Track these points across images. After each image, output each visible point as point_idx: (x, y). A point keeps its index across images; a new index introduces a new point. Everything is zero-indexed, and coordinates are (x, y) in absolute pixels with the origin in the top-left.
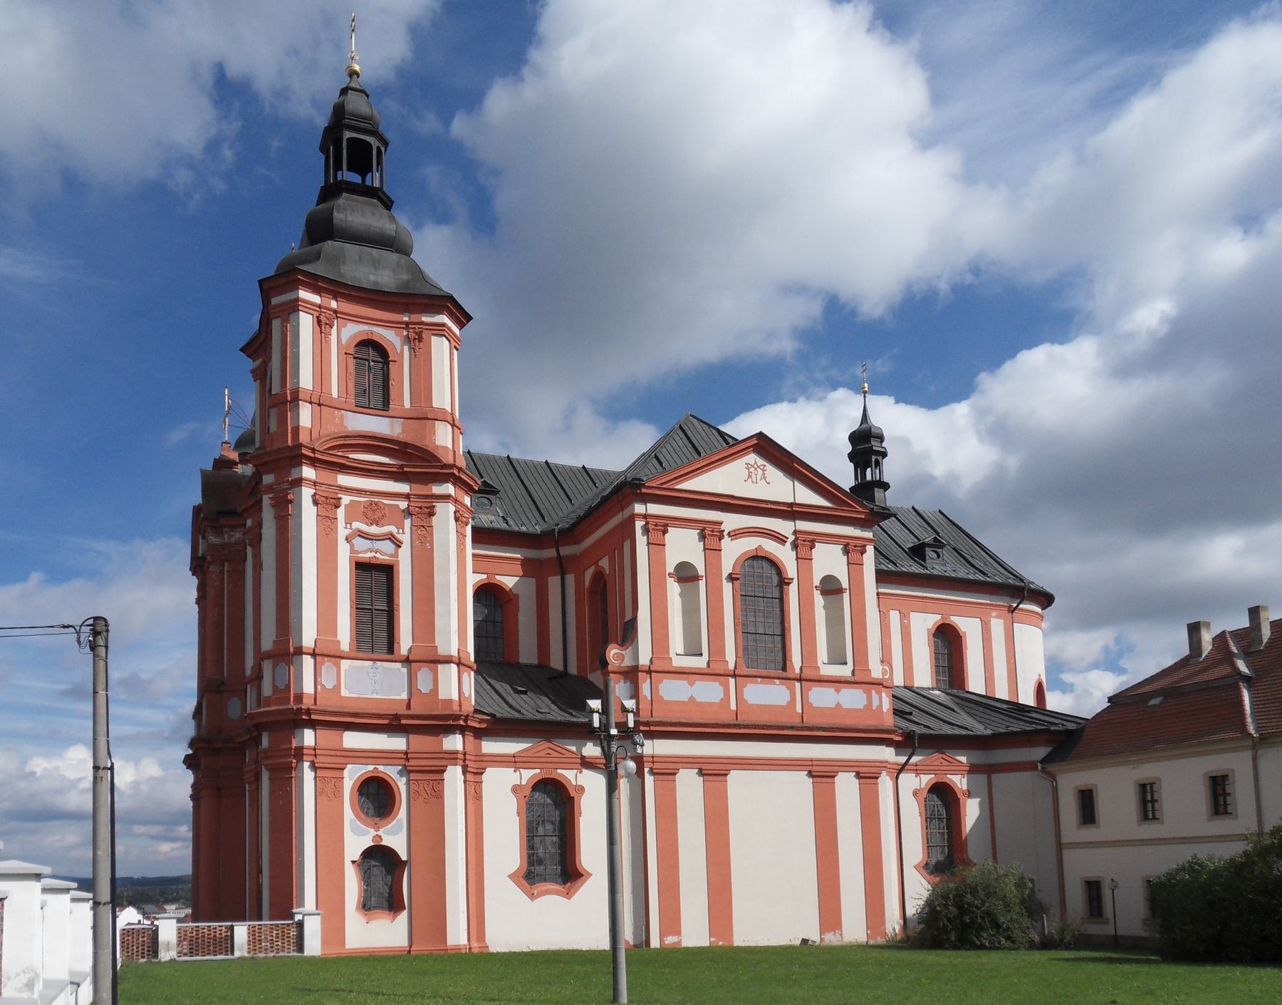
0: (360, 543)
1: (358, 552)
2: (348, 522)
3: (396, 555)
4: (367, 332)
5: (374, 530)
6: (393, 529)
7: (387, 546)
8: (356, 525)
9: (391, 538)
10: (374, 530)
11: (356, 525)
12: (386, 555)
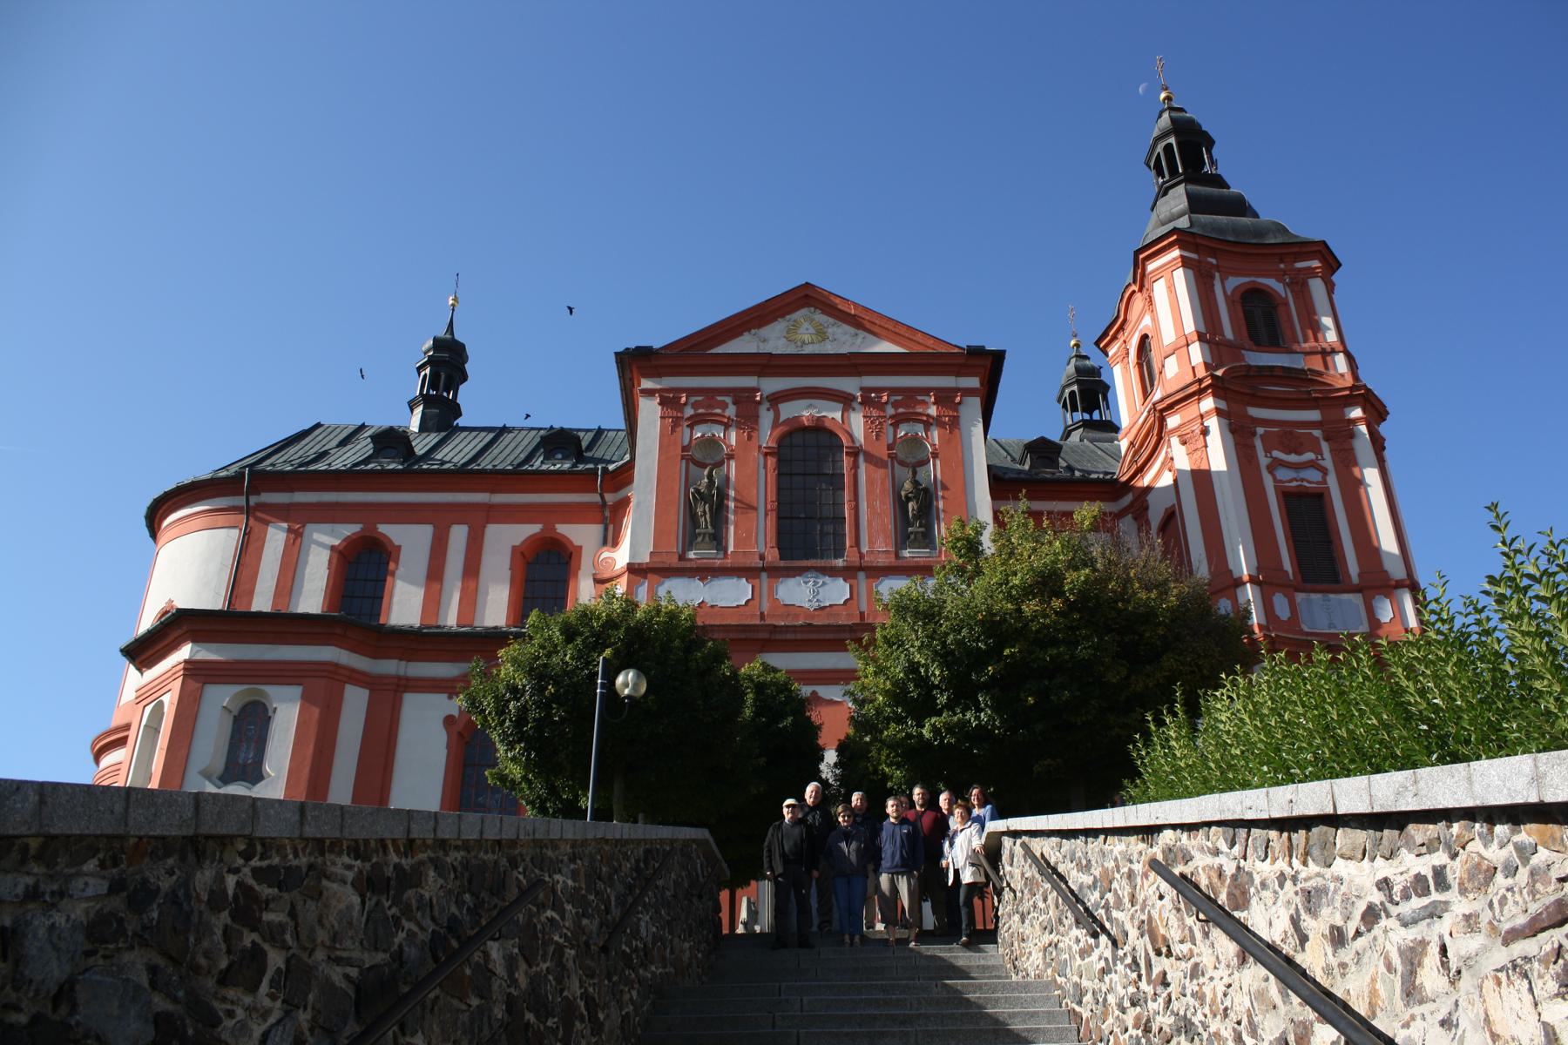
0: (1284, 474)
1: (1281, 481)
2: (1267, 450)
3: (1324, 482)
4: (1249, 283)
5: (1293, 458)
6: (1309, 456)
7: (1313, 475)
8: (1276, 454)
9: (1312, 464)
10: (1293, 458)
11: (1276, 454)
12: (1313, 483)
